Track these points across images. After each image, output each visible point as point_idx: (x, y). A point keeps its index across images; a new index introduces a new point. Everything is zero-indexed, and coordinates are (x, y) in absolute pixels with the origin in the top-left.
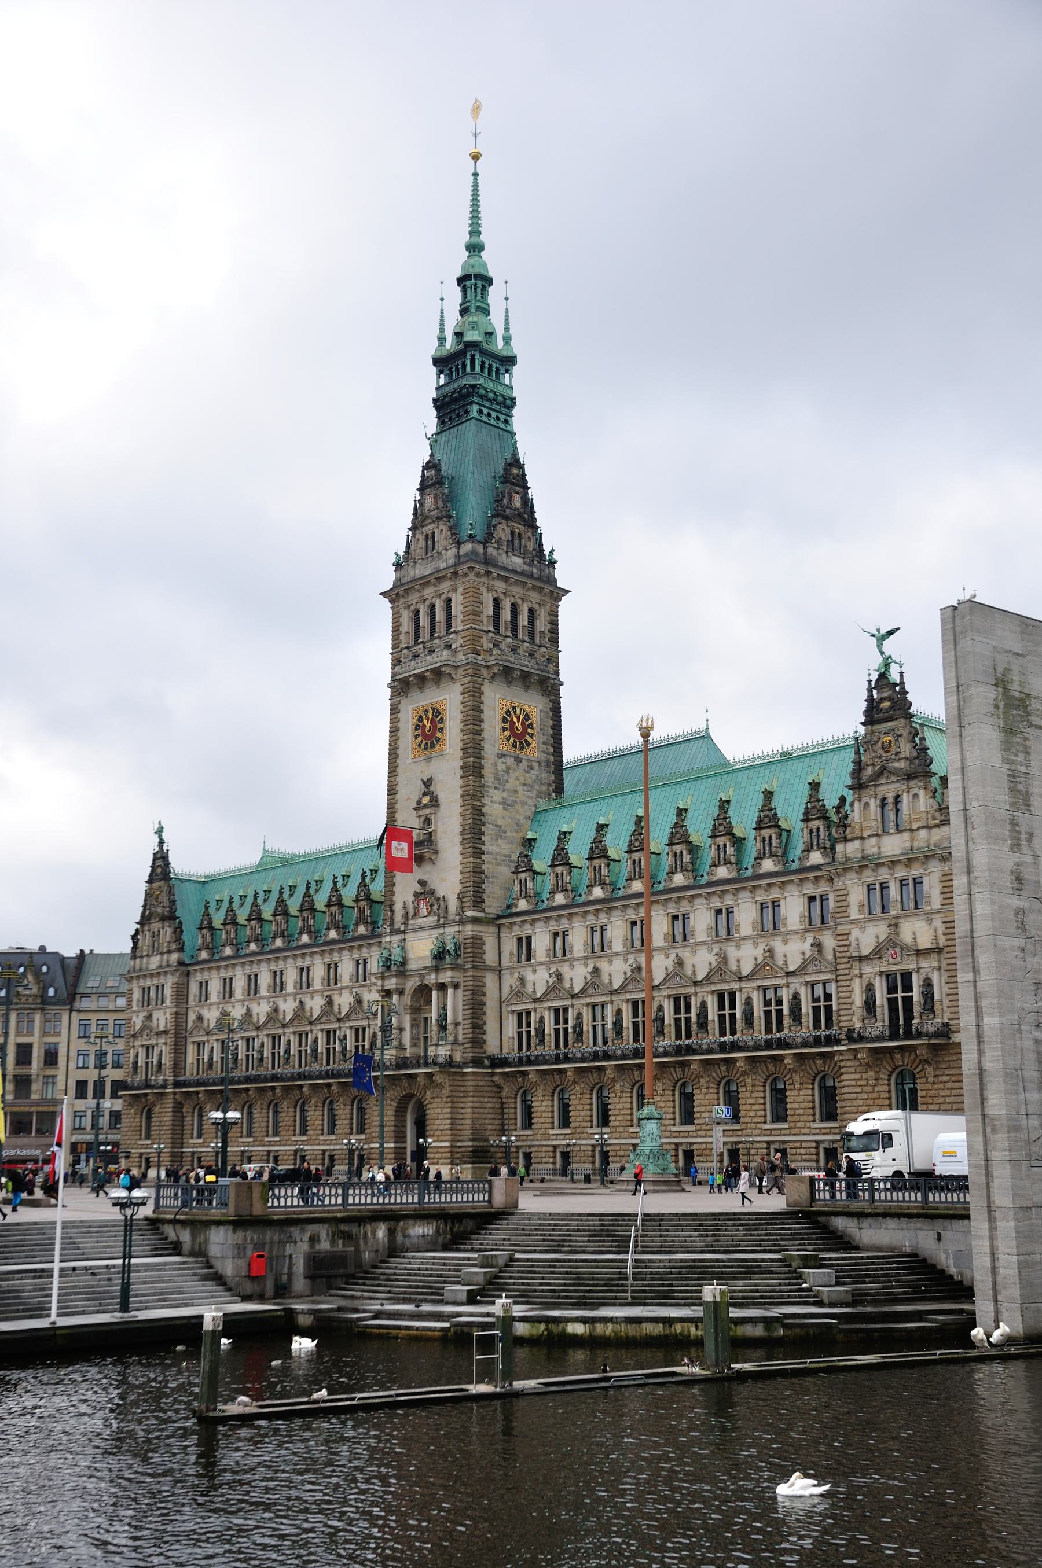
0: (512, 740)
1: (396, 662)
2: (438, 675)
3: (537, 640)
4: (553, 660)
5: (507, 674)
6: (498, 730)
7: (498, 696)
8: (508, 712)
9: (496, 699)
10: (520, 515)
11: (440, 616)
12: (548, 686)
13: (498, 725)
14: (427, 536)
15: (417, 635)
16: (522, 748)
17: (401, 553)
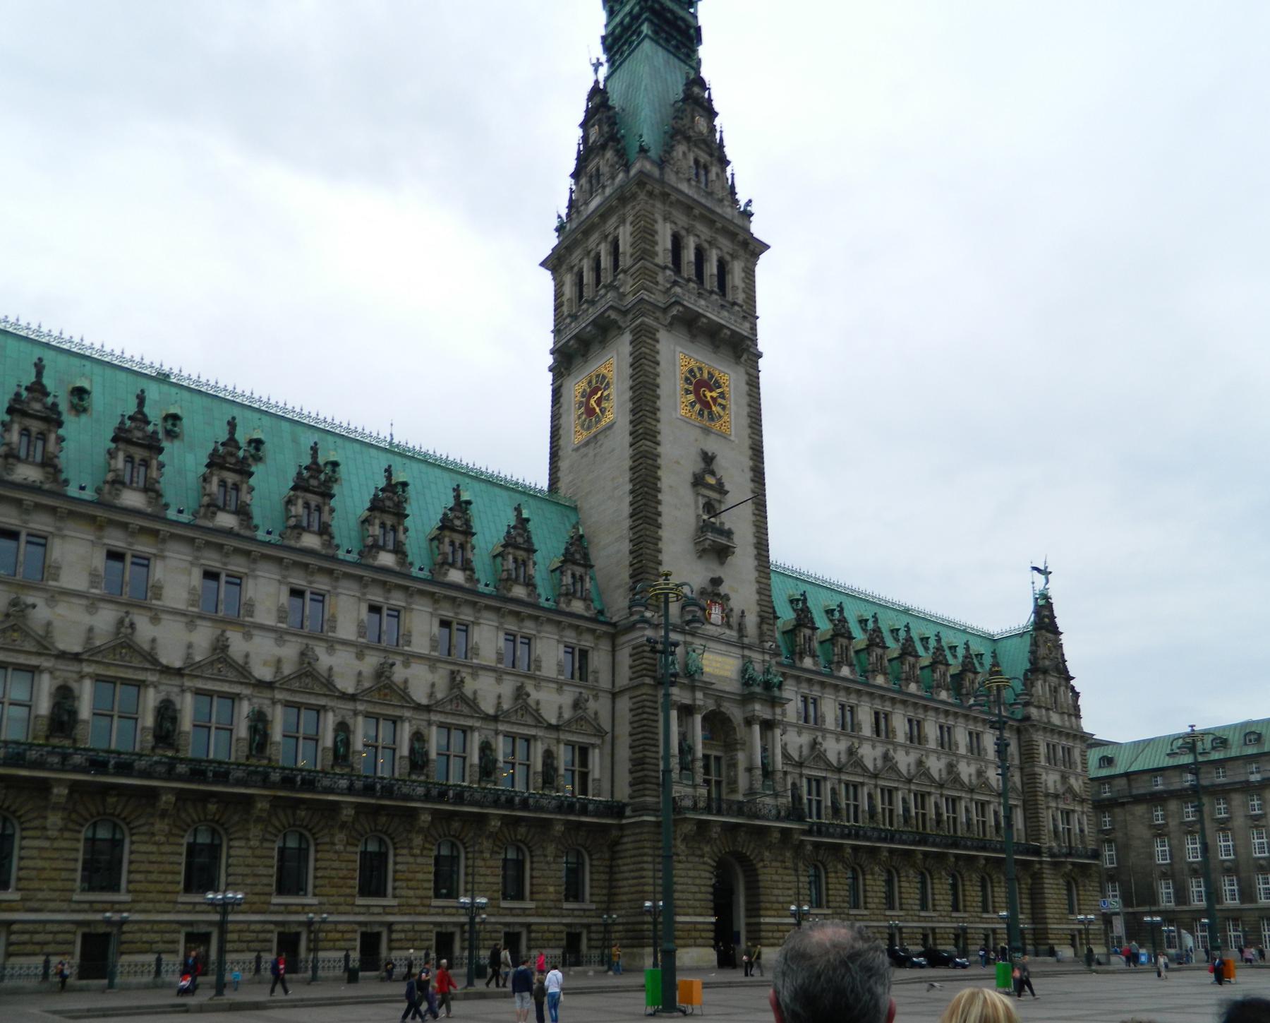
0: (698, 407)
1: (557, 331)
2: (603, 331)
3: (730, 297)
4: (750, 315)
5: (691, 325)
6: (679, 392)
7: (679, 349)
8: (691, 371)
9: (677, 357)
10: (704, 141)
11: (606, 262)
12: (743, 349)
13: (680, 384)
14: (591, 177)
15: (581, 296)
16: (712, 419)
17: (564, 212)
